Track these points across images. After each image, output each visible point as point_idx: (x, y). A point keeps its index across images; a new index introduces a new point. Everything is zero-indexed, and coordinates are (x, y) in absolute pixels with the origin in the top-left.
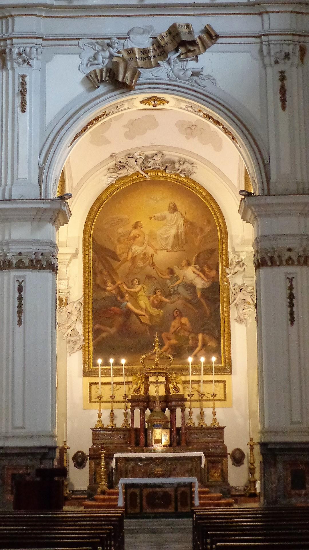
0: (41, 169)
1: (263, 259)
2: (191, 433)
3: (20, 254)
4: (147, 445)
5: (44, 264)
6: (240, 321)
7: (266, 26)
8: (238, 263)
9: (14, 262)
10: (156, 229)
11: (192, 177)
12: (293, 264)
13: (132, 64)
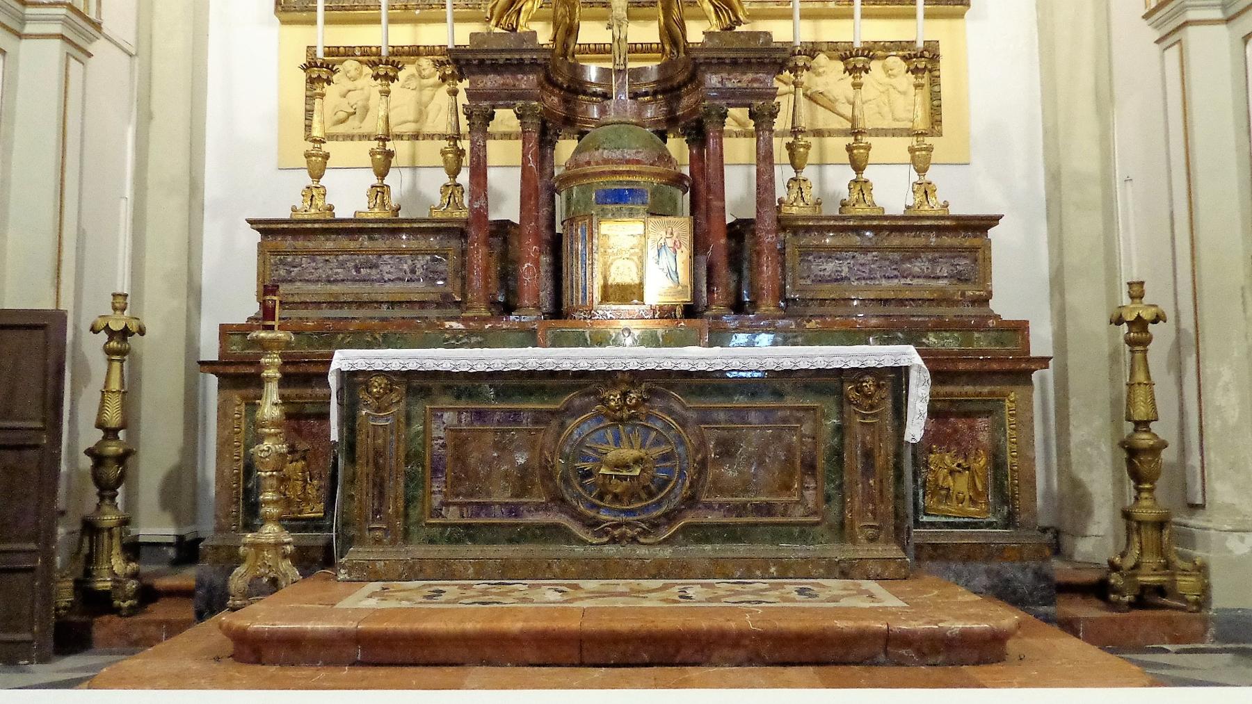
2: (805, 252)
4: (558, 311)
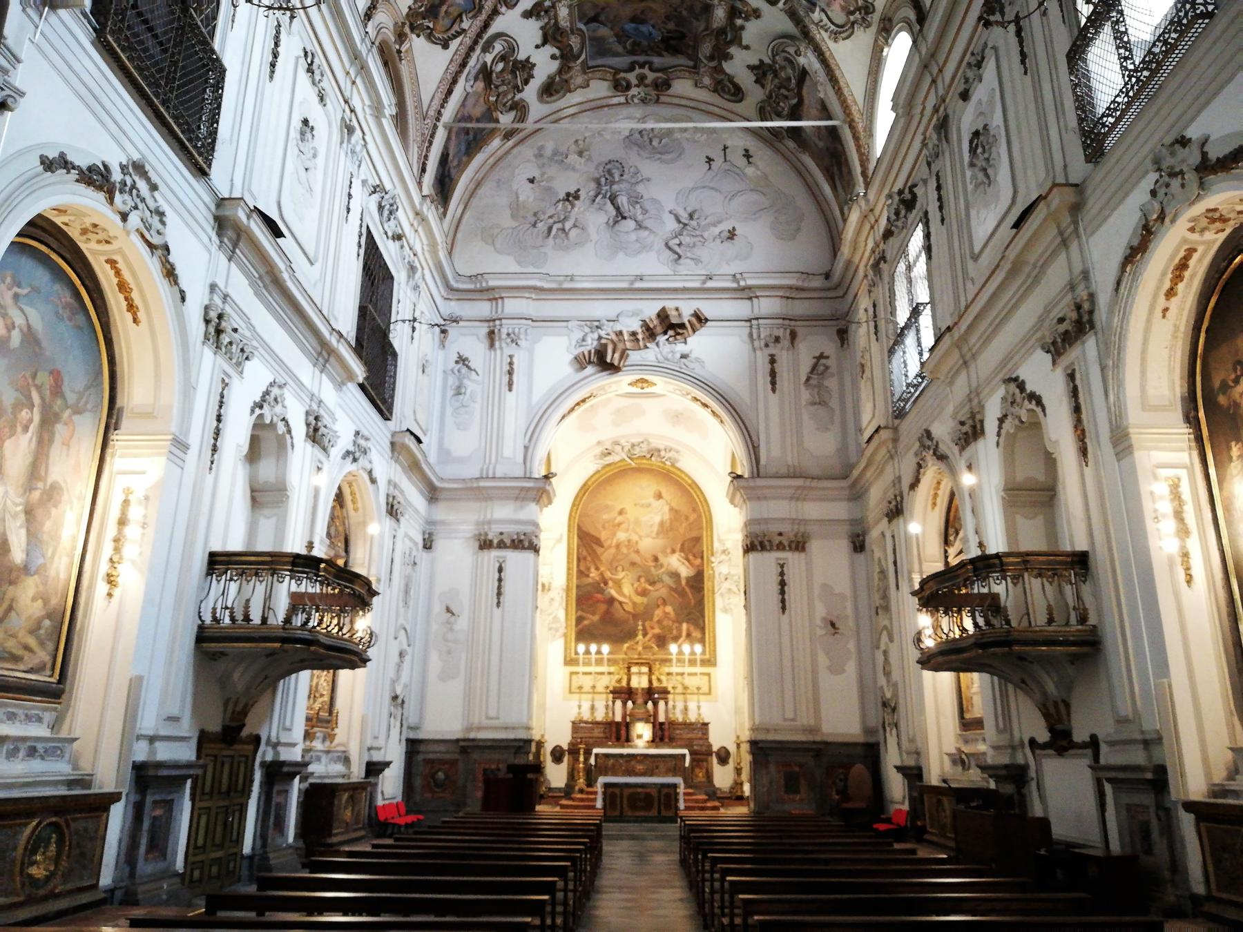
0: (526, 448)
1: (752, 543)
3: (501, 534)
4: (628, 740)
5: (526, 544)
6: (725, 610)
7: (756, 311)
8: (724, 552)
9: (495, 542)
10: (641, 517)
11: (678, 465)
12: (784, 549)
13: (620, 346)
